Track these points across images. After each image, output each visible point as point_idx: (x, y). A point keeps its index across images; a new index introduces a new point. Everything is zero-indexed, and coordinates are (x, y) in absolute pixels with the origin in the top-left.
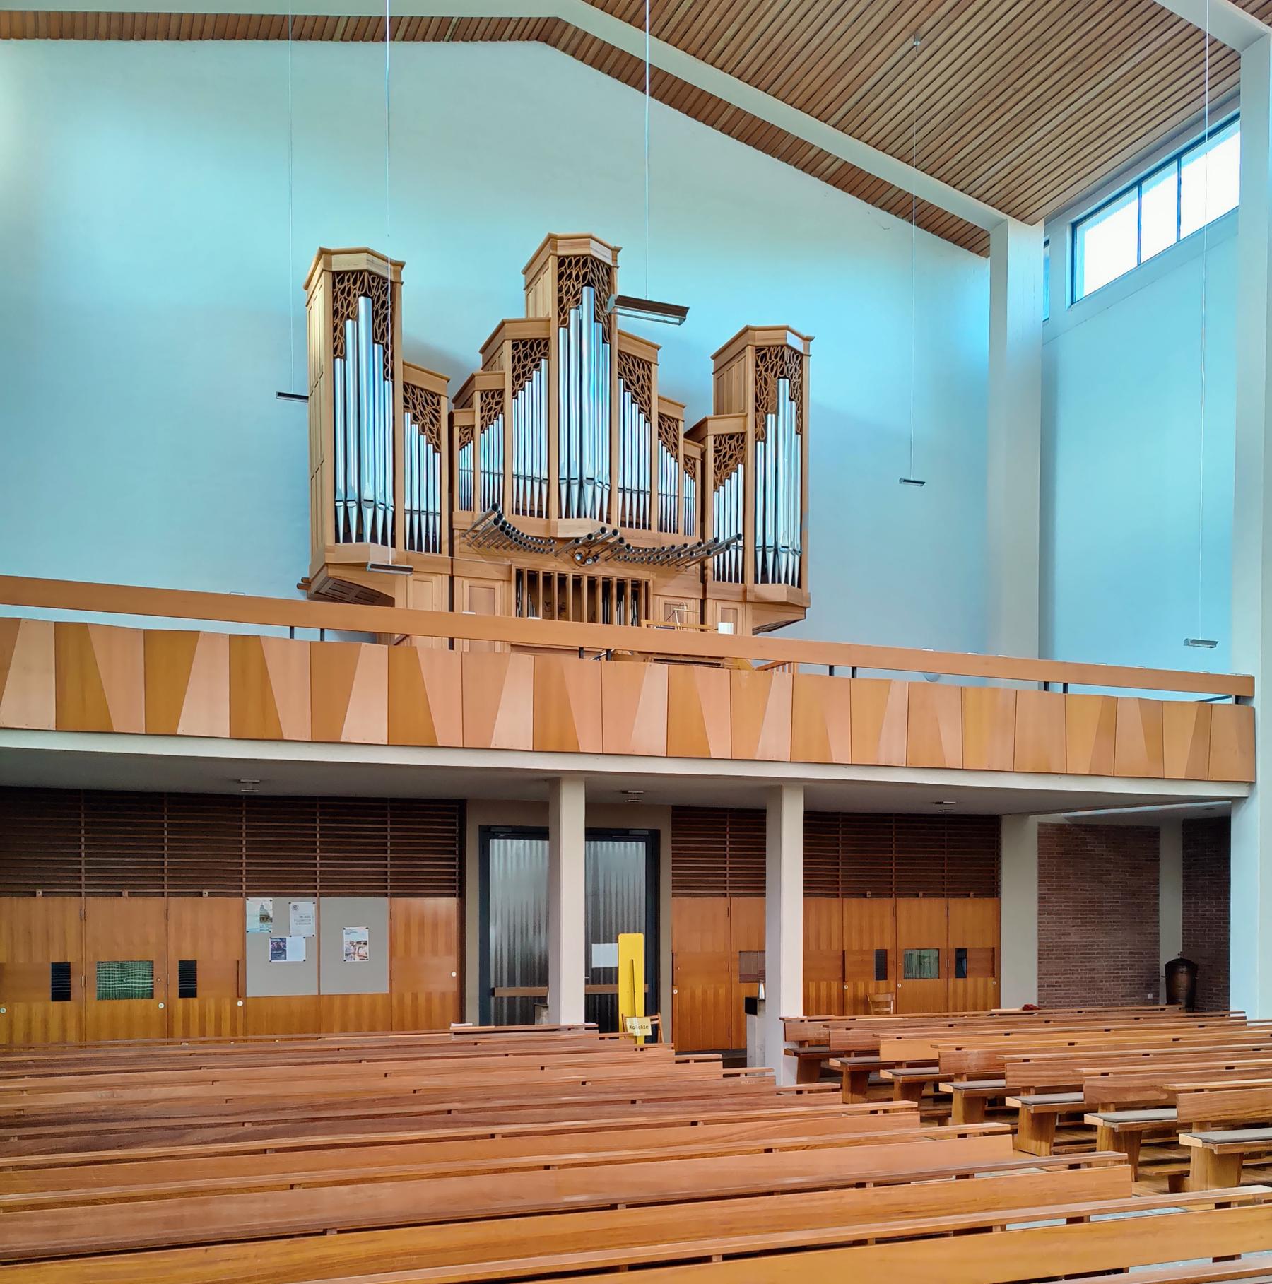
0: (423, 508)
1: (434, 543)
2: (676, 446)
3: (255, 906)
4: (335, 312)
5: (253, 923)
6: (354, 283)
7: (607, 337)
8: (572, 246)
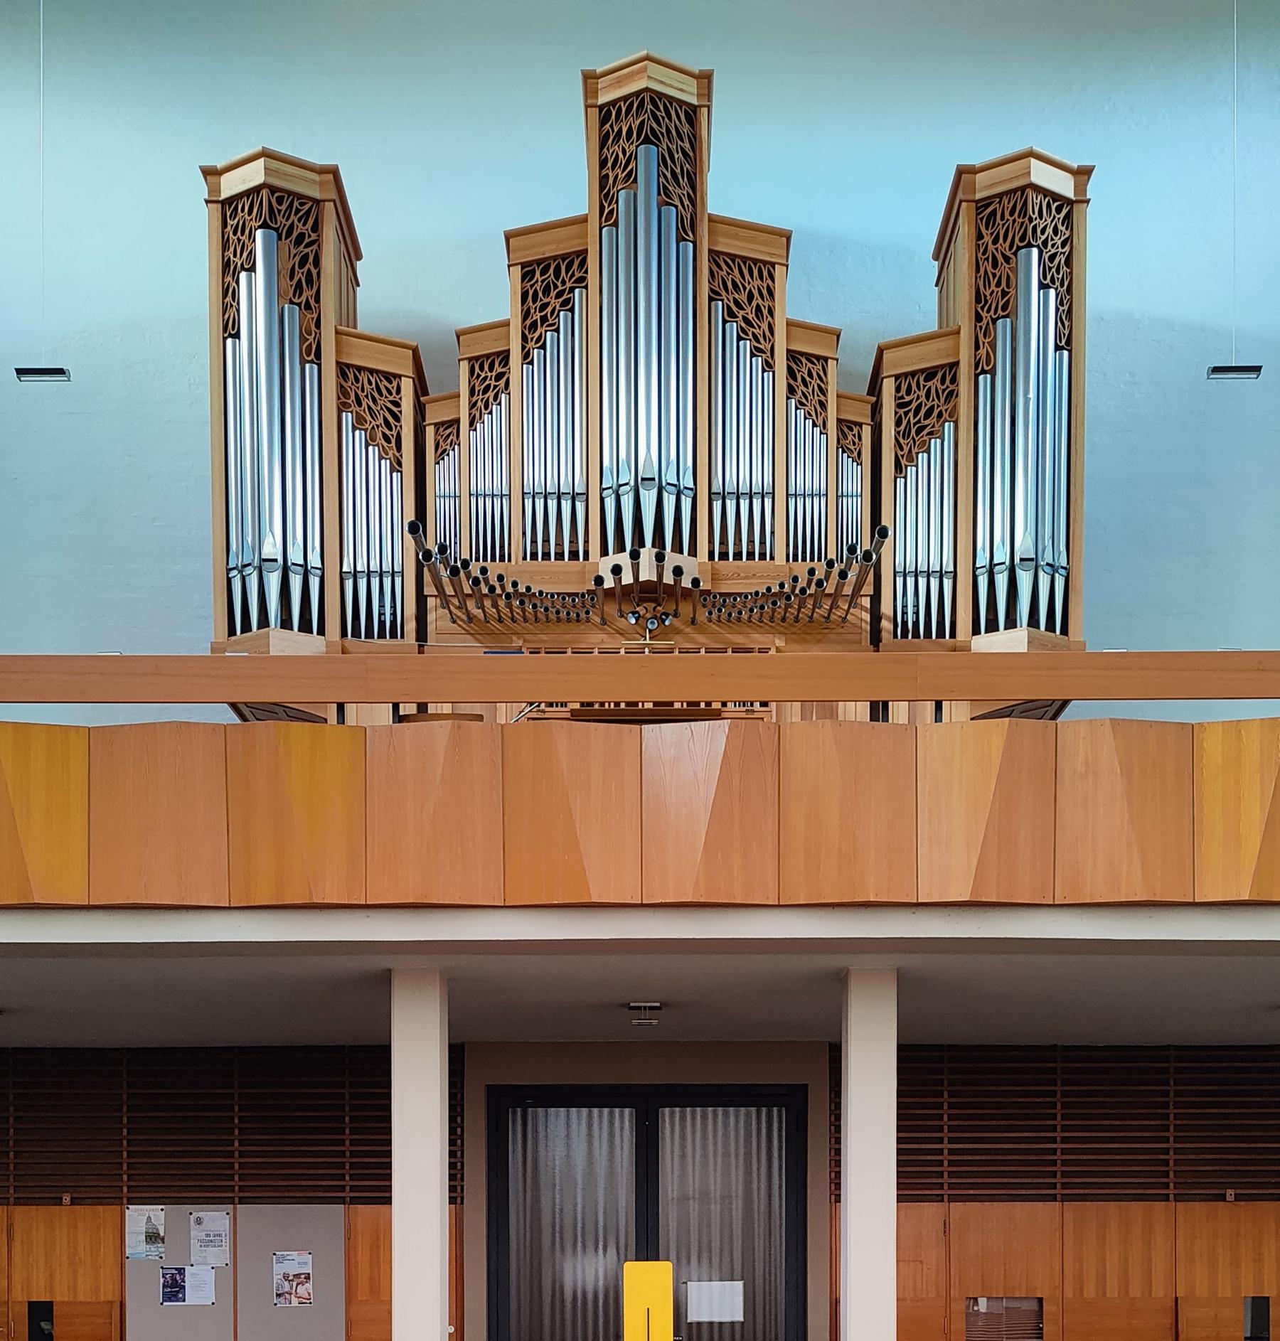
0: (374, 566)
1: (382, 624)
2: (823, 405)
3: (139, 1218)
4: (226, 265)
5: (135, 1245)
6: (250, 213)
7: (687, 228)
8: (619, 83)
